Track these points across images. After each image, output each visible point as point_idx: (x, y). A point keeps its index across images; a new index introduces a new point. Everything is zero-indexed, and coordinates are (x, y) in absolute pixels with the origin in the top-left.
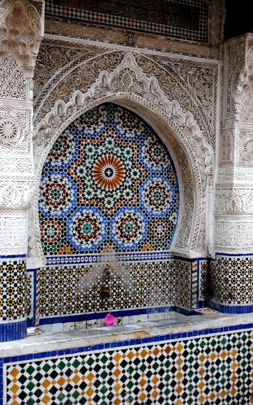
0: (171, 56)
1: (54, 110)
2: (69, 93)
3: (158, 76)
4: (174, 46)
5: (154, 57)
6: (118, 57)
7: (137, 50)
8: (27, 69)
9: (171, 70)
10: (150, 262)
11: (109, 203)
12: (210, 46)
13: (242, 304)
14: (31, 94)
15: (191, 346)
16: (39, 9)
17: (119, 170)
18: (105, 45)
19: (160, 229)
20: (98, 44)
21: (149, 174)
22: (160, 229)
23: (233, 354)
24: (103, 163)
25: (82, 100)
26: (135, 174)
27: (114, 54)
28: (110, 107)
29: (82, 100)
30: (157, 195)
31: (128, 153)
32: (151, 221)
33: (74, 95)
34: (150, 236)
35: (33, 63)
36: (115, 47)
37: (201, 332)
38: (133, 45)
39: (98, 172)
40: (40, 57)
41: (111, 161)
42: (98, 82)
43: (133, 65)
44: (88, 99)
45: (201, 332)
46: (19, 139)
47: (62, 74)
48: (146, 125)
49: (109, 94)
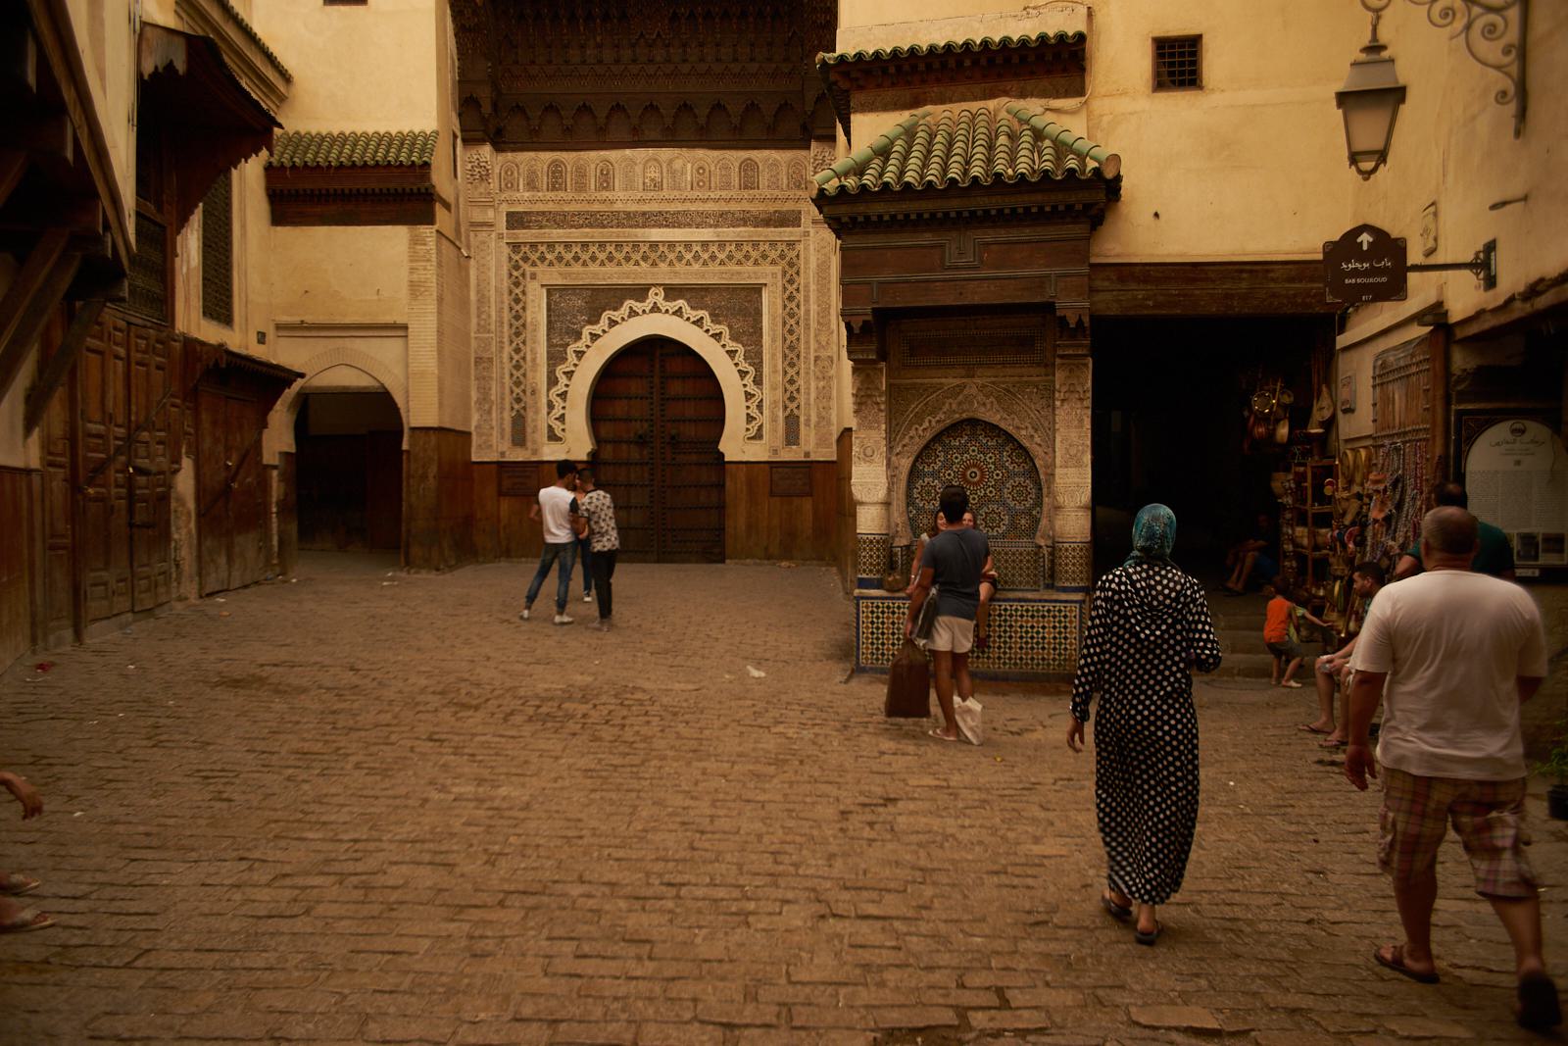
0: (1007, 379)
1: (912, 433)
2: (923, 420)
3: (996, 398)
4: (1009, 371)
5: (993, 383)
6: (962, 387)
7: (978, 381)
8: (881, 411)
9: (1008, 391)
10: (1013, 549)
11: (974, 499)
12: (1046, 366)
13: (1067, 584)
14: (883, 427)
15: (1006, 610)
16: (882, 372)
17: (982, 472)
18: (951, 380)
19: (1023, 522)
20: (943, 380)
21: (1011, 475)
22: (1023, 522)
23: (1049, 622)
24: (967, 468)
25: (933, 424)
26: (998, 475)
27: (958, 386)
28: (974, 423)
29: (933, 424)
30: (1020, 493)
31: (990, 458)
32: (1014, 516)
33: (927, 421)
34: (1013, 526)
35: (883, 407)
36: (957, 381)
37: (1014, 600)
38: (973, 377)
39: (964, 475)
40: (889, 403)
41: (975, 466)
42: (946, 407)
43: (974, 391)
44: (938, 421)
45: (1014, 600)
46: (876, 456)
47: (915, 407)
48: (1006, 433)
49: (957, 416)
